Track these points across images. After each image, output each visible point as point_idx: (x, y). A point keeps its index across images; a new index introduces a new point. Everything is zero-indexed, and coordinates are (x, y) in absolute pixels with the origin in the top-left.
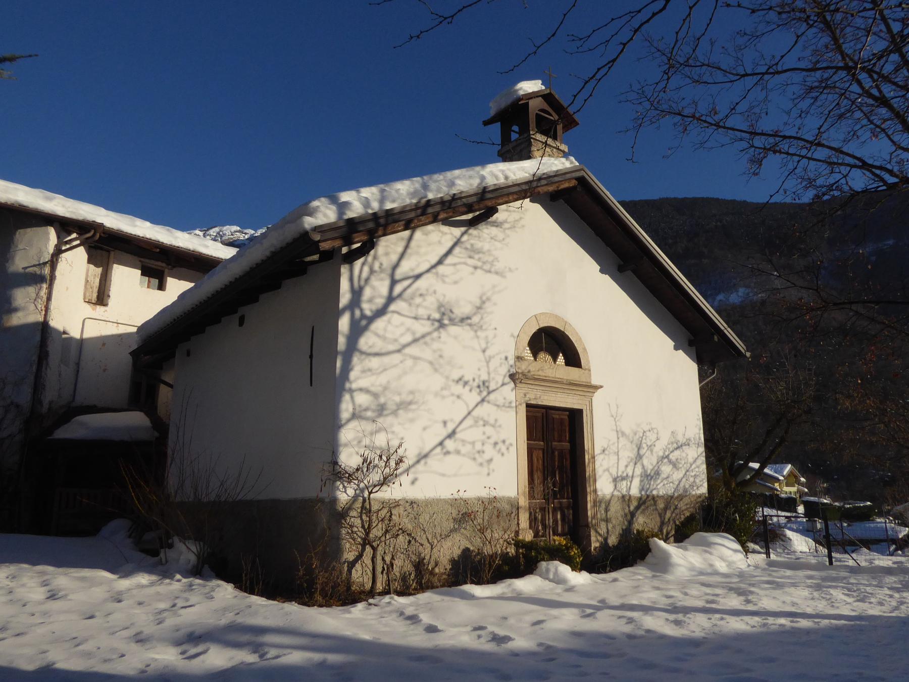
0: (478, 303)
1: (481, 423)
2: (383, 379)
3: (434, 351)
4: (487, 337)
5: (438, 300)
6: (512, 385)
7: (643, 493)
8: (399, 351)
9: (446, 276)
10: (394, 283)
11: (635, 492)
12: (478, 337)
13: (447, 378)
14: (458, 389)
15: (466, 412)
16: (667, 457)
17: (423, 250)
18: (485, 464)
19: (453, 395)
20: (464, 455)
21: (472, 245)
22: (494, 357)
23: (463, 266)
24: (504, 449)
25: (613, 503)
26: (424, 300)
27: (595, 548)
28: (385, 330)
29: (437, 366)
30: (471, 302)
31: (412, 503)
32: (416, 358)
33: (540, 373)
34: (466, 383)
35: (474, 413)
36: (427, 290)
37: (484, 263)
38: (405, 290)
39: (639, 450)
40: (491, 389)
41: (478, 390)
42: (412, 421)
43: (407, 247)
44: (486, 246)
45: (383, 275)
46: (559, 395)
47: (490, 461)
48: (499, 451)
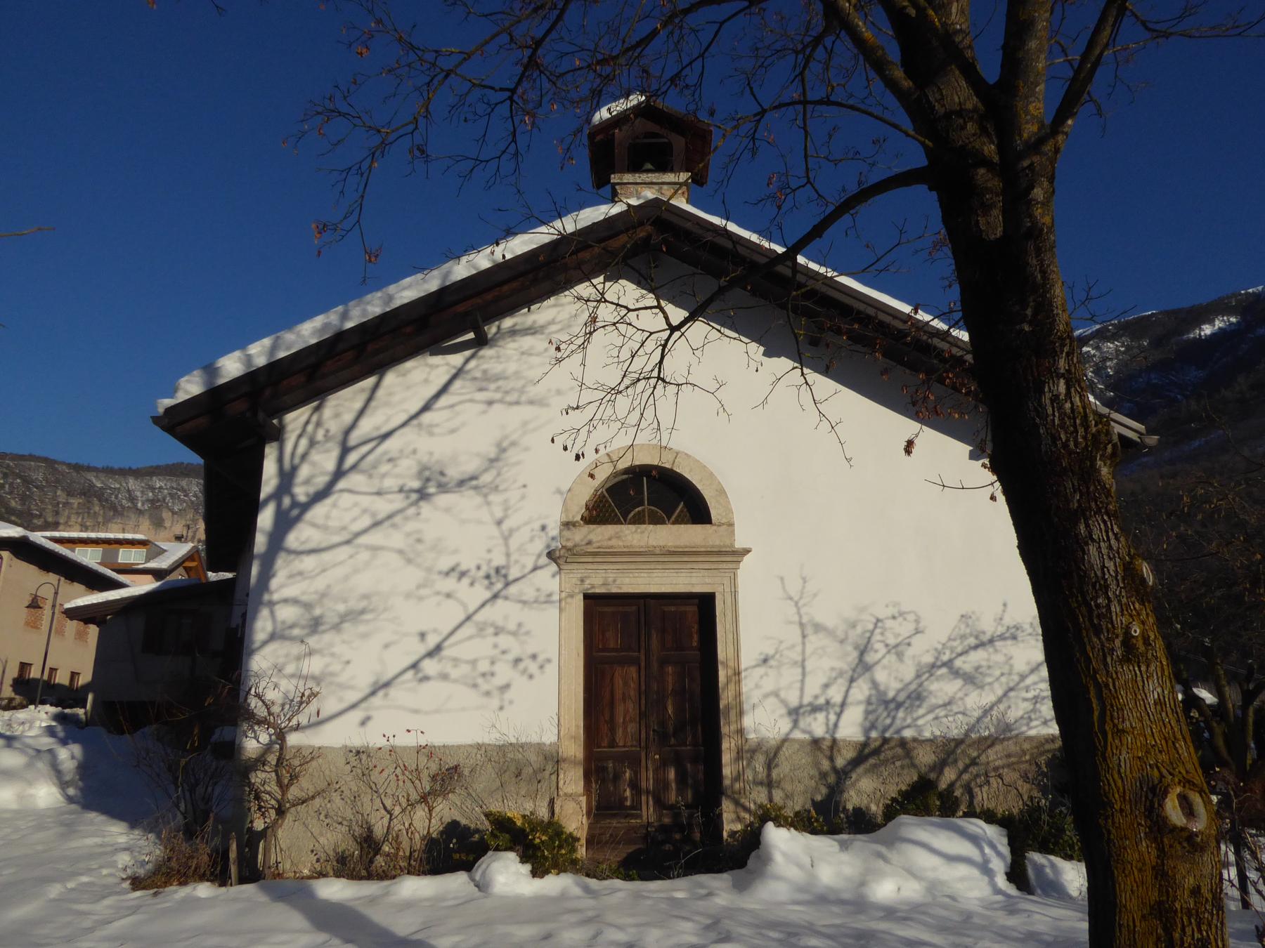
0: (492, 453)
1: (491, 630)
2: (320, 584)
3: (408, 535)
4: (506, 501)
5: (419, 462)
6: (554, 567)
7: (874, 734)
8: (348, 542)
9: (437, 425)
10: (345, 450)
11: (851, 728)
12: (488, 504)
13: (429, 570)
14: (450, 584)
15: (462, 617)
16: (948, 664)
17: (396, 398)
18: (496, 693)
19: (438, 593)
20: (455, 681)
21: (485, 372)
22: (518, 528)
23: (468, 405)
24: (533, 667)
25: (786, 751)
26: (395, 466)
27: (733, 834)
28: (327, 517)
29: (411, 556)
30: (478, 455)
31: (358, 752)
32: (375, 549)
33: (614, 542)
34: (463, 574)
35: (479, 617)
36: (401, 451)
37: (507, 392)
38: (363, 457)
39: (862, 653)
40: (511, 578)
41: (486, 582)
42: (365, 636)
43: (370, 399)
44: (512, 367)
45: (329, 445)
46: (656, 574)
47: (506, 687)
48: (524, 671)
